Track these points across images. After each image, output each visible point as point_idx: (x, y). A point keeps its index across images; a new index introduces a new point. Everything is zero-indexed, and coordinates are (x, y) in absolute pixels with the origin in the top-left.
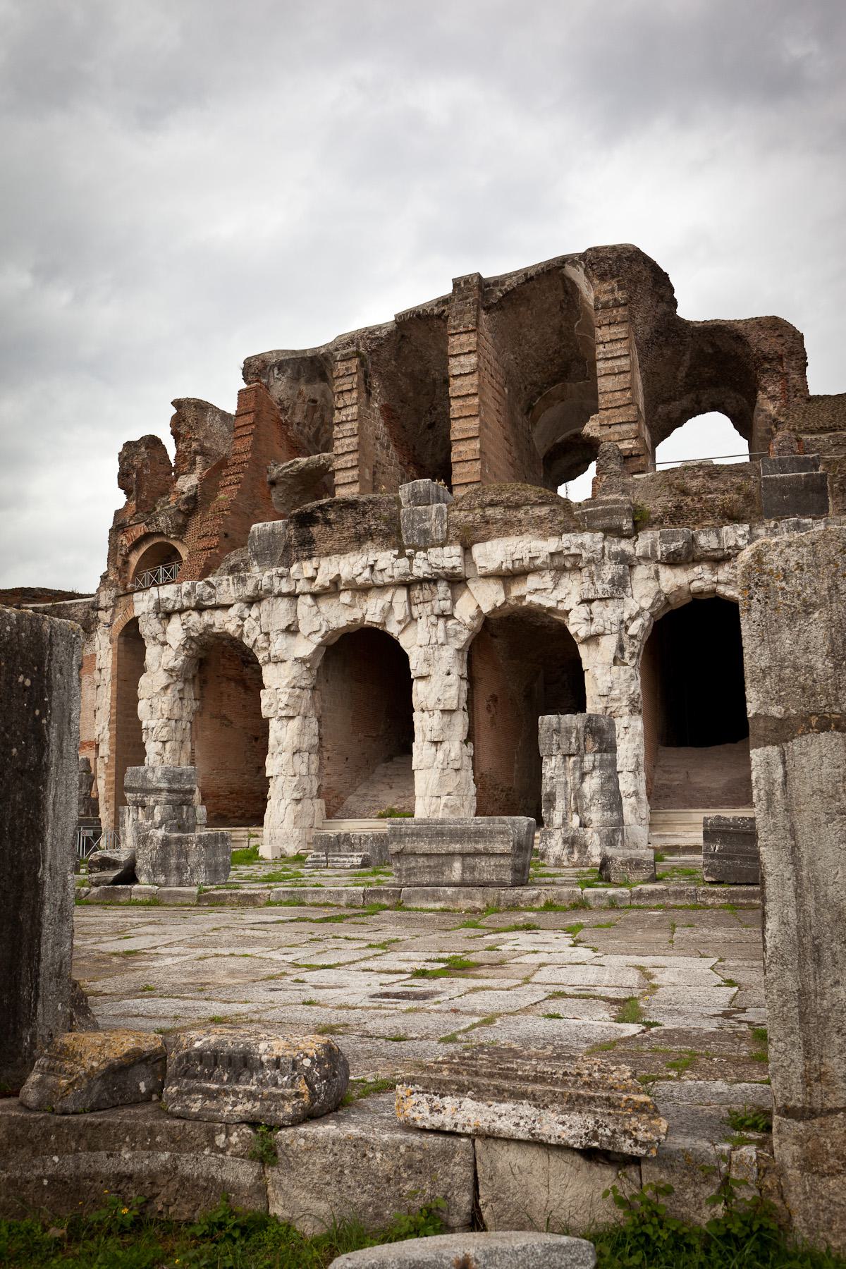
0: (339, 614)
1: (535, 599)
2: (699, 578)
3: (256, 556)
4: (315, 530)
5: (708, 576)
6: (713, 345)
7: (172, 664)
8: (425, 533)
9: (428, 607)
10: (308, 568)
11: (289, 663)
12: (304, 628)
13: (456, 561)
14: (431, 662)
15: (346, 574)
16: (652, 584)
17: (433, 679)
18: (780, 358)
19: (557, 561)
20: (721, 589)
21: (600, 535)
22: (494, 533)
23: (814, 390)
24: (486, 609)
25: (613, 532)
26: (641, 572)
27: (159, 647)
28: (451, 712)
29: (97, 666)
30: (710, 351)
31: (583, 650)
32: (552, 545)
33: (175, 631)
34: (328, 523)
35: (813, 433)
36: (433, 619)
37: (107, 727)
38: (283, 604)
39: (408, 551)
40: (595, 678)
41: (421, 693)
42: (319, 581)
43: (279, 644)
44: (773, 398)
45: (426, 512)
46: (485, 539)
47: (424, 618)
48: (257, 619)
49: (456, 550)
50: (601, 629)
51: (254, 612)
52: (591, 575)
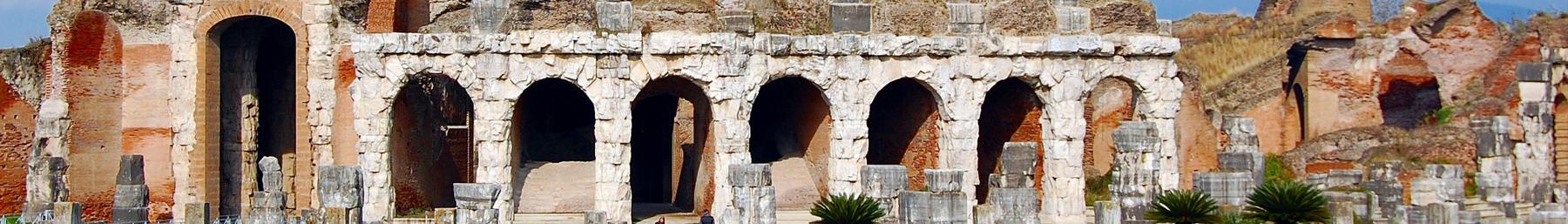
0: (540, 70)
1: (689, 73)
2: (791, 67)
3: (478, 22)
4: (535, 12)
5: (797, 66)
7: (389, 95)
8: (616, 22)
9: (613, 71)
10: (525, 36)
11: (502, 102)
12: (513, 77)
13: (638, 44)
14: (615, 110)
15: (556, 45)
16: (762, 67)
17: (616, 122)
19: (704, 50)
20: (805, 75)
21: (735, 34)
22: (665, 27)
24: (654, 77)
25: (745, 33)
26: (756, 59)
27: (377, 79)
28: (625, 144)
29: (175, 58)
31: (715, 108)
32: (705, 38)
33: (397, 71)
34: (547, 9)
36: (617, 80)
37: (192, 118)
38: (499, 59)
39: (604, 34)
40: (724, 127)
41: (601, 130)
42: (529, 47)
43: (494, 88)
45: (617, 6)
46: (658, 30)
47: (608, 79)
48: (473, 68)
49: (639, 35)
50: (730, 96)
51: (472, 61)
52: (726, 60)
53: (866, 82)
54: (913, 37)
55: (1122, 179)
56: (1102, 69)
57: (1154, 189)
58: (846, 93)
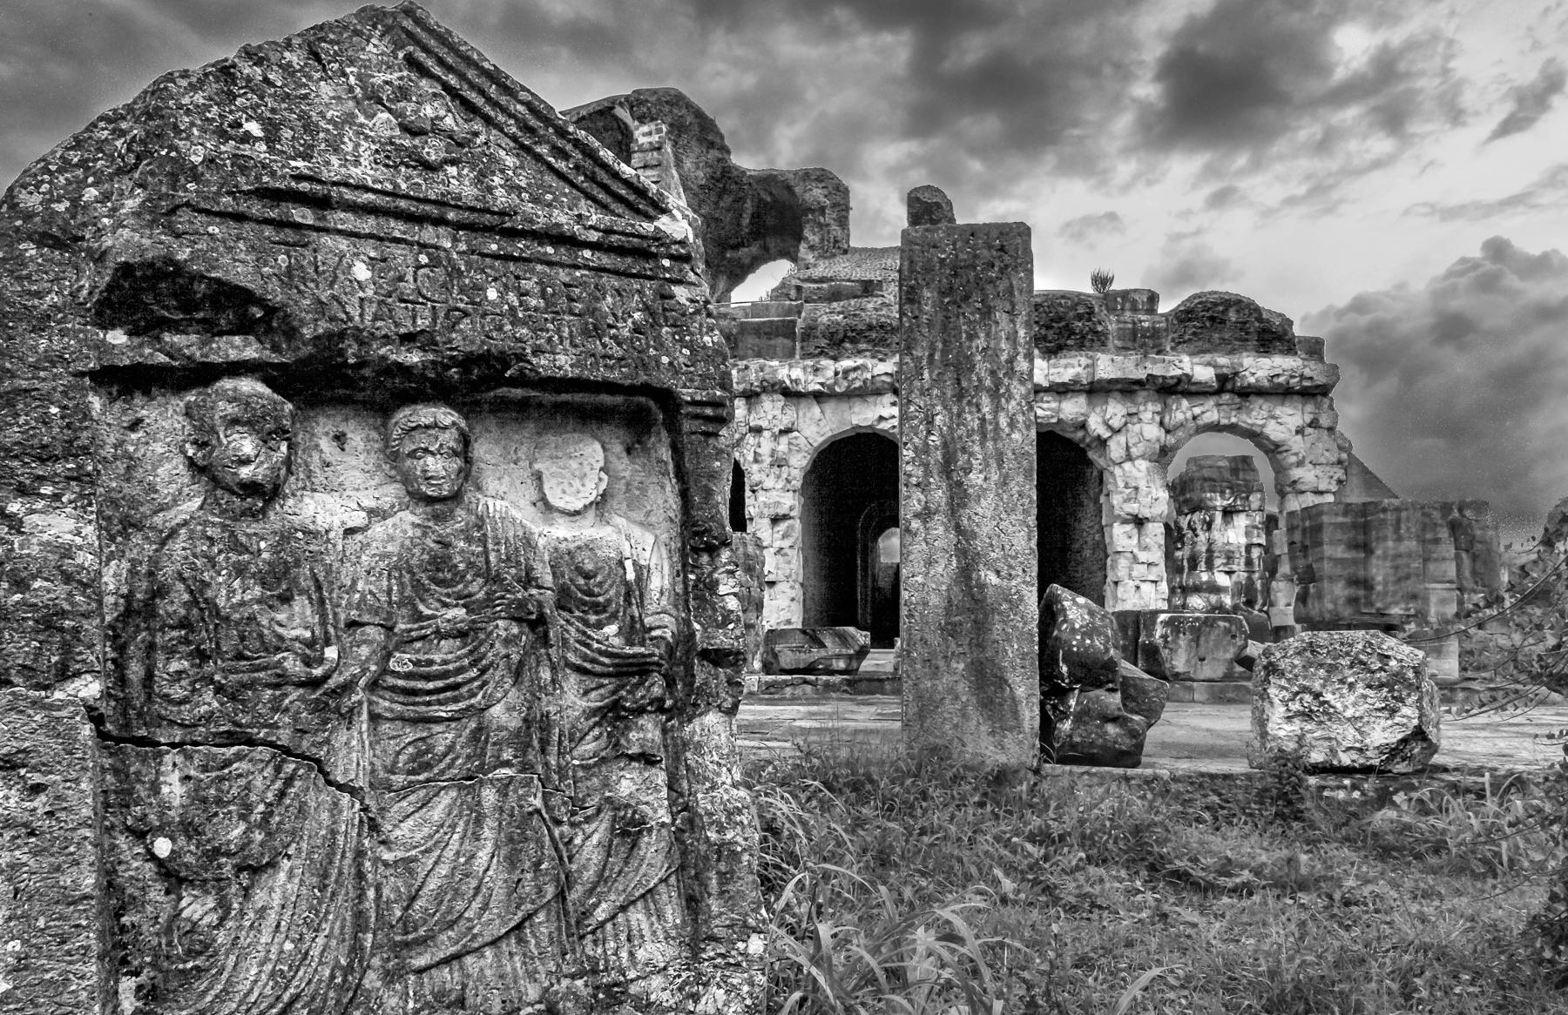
6: (771, 194)
18: (822, 210)
23: (854, 243)
30: (769, 199)
35: (815, 281)
44: (812, 248)
53: (795, 434)
54: (860, 361)
55: (1185, 563)
56: (1197, 411)
57: (1249, 579)
58: (758, 450)
